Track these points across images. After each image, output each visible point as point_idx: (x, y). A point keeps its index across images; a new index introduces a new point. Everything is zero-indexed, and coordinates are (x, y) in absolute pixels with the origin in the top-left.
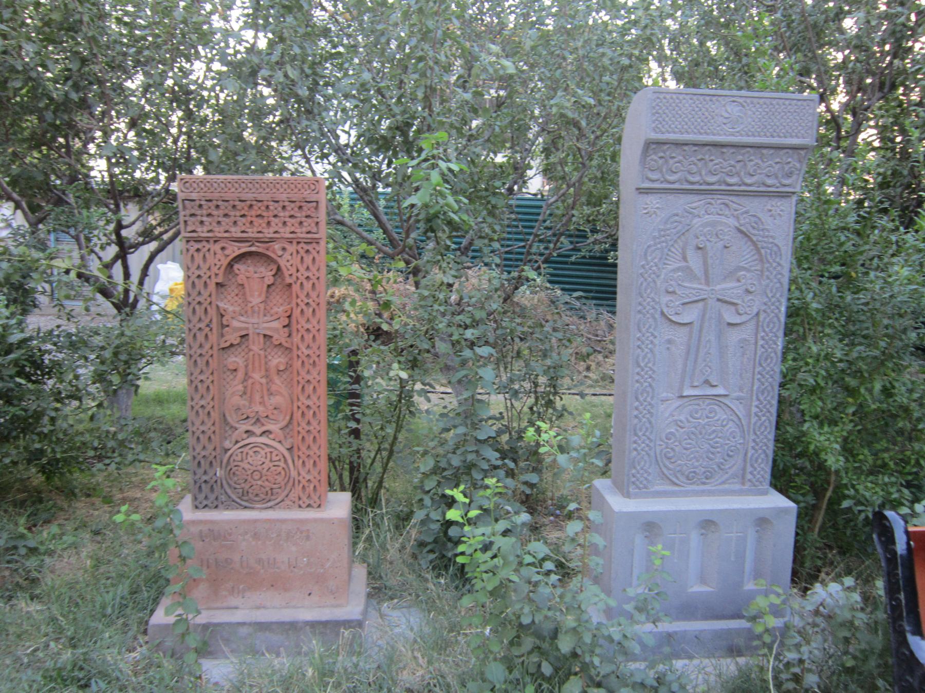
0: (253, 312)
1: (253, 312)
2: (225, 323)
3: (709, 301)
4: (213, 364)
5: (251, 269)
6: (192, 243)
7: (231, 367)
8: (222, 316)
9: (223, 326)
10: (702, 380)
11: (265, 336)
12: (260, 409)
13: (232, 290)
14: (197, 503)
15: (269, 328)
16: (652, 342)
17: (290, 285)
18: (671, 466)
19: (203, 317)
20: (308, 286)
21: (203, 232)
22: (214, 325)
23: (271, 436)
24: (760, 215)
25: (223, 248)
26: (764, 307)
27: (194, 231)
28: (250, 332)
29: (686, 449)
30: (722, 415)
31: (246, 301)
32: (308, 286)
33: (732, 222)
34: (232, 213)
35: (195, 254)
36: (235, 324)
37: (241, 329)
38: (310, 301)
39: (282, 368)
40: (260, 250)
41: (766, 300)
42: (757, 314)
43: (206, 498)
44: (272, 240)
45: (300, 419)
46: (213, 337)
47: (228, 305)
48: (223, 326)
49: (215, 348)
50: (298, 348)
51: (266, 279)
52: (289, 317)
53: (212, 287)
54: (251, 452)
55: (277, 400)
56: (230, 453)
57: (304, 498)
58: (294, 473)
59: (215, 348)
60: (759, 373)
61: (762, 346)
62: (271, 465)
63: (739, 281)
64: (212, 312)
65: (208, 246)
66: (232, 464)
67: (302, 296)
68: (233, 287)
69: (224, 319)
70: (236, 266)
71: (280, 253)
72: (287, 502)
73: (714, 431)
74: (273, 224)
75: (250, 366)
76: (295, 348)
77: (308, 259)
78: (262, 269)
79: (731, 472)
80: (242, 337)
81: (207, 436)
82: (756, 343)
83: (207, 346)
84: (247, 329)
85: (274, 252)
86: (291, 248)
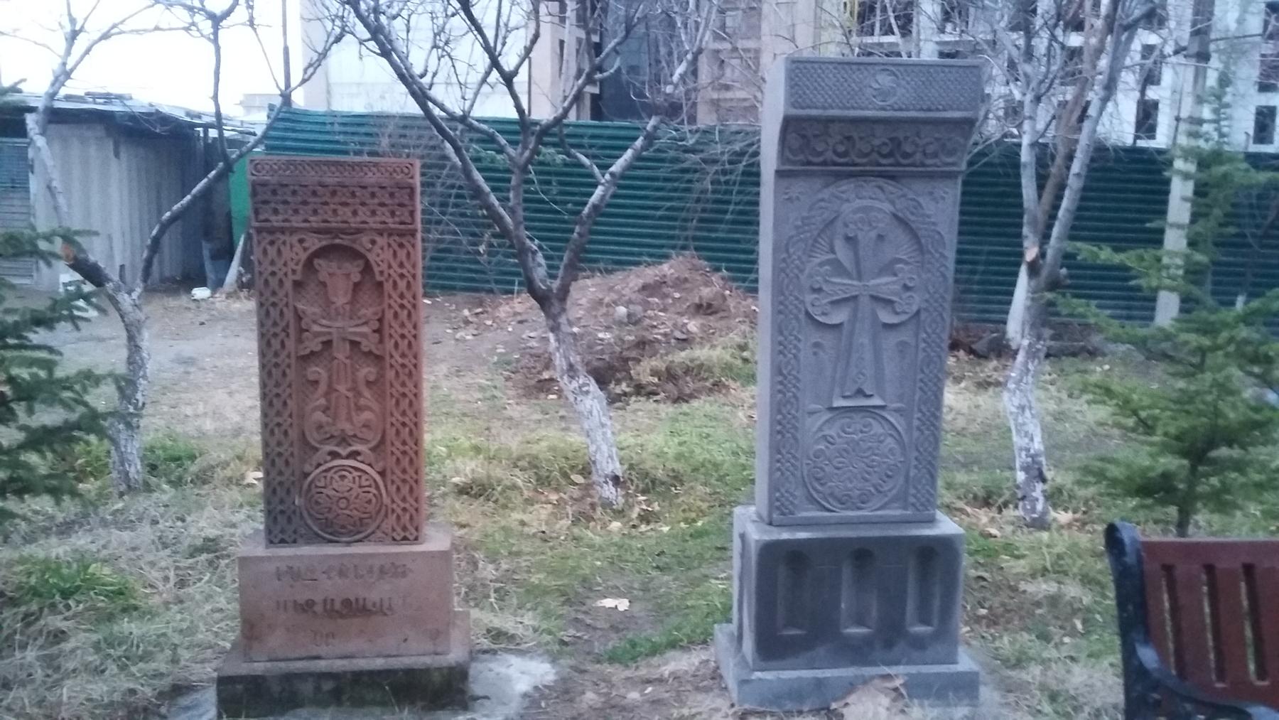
0: (338, 314)
2: (304, 327)
3: (861, 299)
5: (334, 264)
6: (264, 234)
7: (311, 378)
8: (300, 319)
9: (302, 331)
10: (855, 388)
12: (347, 427)
15: (355, 334)
16: (795, 347)
17: (380, 284)
18: (819, 488)
20: (402, 285)
21: (276, 221)
22: (292, 331)
24: (921, 200)
26: (924, 305)
27: (267, 220)
28: (335, 337)
29: (838, 468)
30: (877, 428)
31: (329, 303)
32: (402, 285)
33: (887, 207)
34: (312, 200)
35: (269, 247)
36: (316, 328)
38: (405, 302)
39: (372, 378)
40: (345, 243)
41: (927, 296)
42: (918, 313)
43: (282, 531)
44: (359, 231)
45: (394, 438)
46: (290, 344)
48: (302, 331)
50: (392, 356)
53: (288, 284)
55: (366, 415)
56: (310, 479)
57: (399, 530)
58: (386, 500)
59: (293, 355)
60: (921, 380)
61: (924, 350)
62: (360, 490)
63: (895, 275)
64: (289, 315)
65: (283, 238)
66: (314, 490)
67: (395, 296)
70: (316, 261)
72: (379, 534)
73: (870, 448)
74: (360, 213)
75: (334, 378)
76: (387, 358)
77: (402, 254)
78: (347, 265)
79: (890, 495)
80: (323, 343)
81: (283, 459)
82: (917, 346)
84: (330, 333)
85: (361, 244)
86: (381, 241)
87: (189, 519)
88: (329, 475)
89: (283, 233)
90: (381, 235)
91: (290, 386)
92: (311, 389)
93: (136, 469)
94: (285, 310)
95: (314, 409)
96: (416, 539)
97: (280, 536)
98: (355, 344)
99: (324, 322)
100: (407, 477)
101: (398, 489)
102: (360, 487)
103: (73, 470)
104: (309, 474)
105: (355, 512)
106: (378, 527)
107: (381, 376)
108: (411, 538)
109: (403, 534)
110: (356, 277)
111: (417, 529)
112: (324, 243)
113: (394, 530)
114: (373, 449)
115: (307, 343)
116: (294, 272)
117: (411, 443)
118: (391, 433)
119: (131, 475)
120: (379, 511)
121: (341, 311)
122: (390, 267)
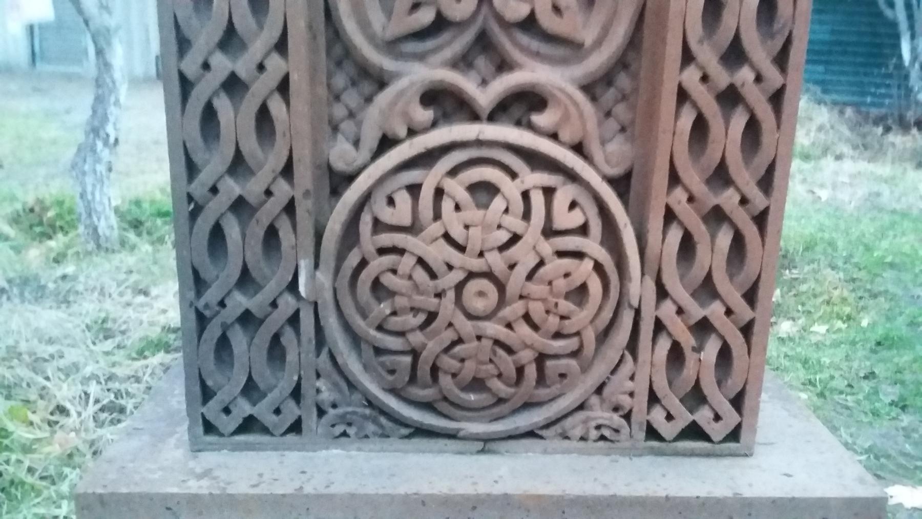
14: (212, 410)
23: (541, 119)
43: (251, 389)
54: (456, 188)
58: (640, 288)
62: (547, 248)
72: (600, 414)
87: (154, 291)
88: (430, 178)
93: (108, 225)
96: (734, 435)
97: (244, 408)
100: (729, 199)
101: (687, 246)
102: (549, 232)
103: (41, 223)
104: (350, 178)
105: (524, 329)
106: (599, 390)
108: (717, 431)
109: (684, 418)
111: (737, 402)
113: (653, 399)
114: (590, 88)
119: (100, 231)
120: (604, 335)
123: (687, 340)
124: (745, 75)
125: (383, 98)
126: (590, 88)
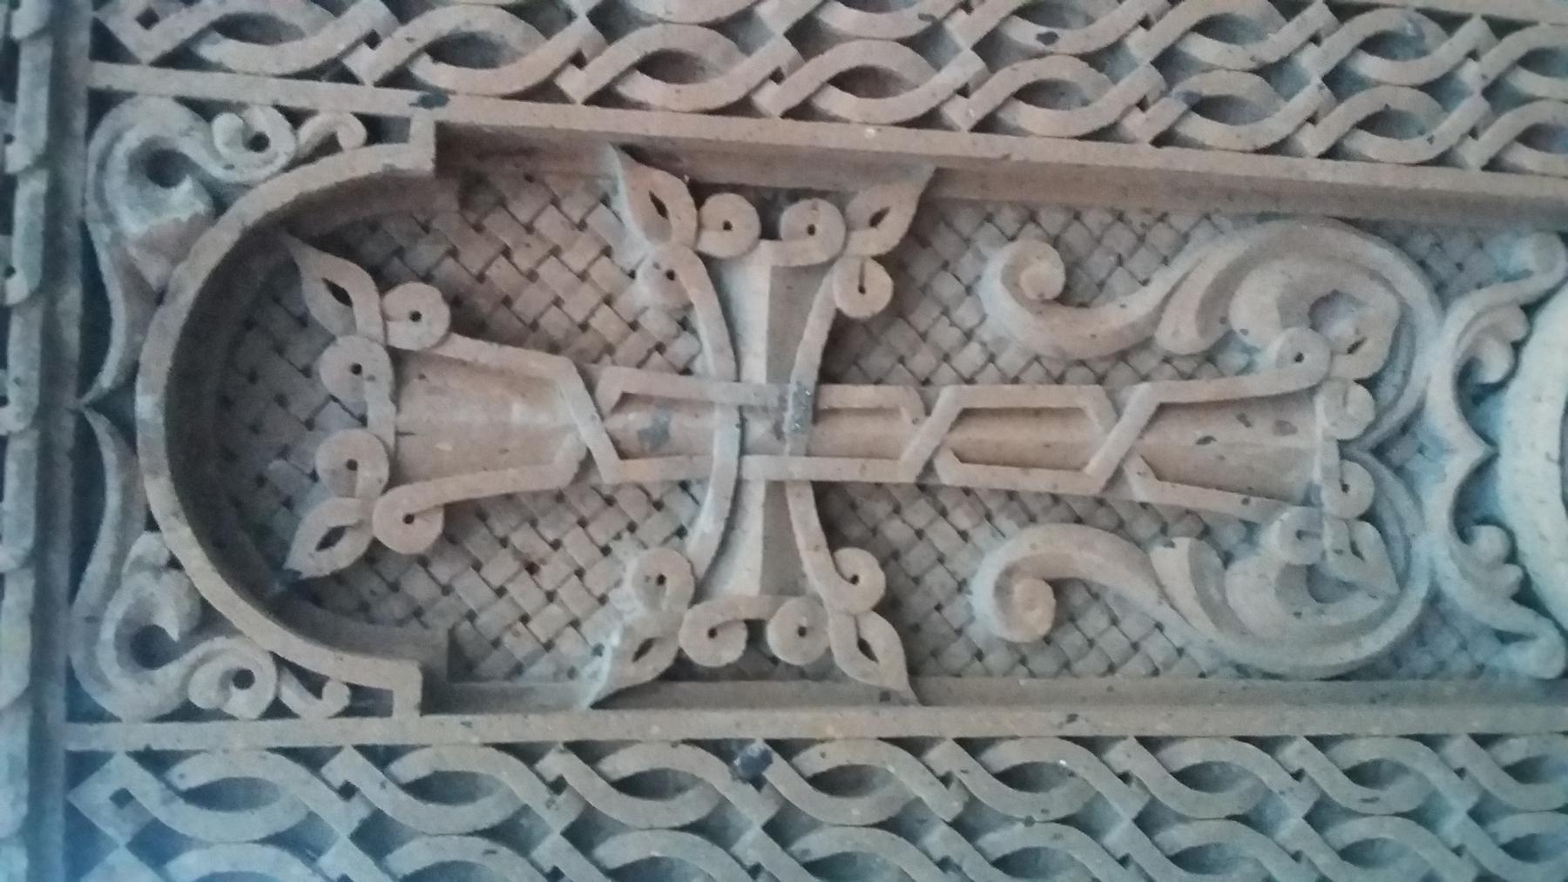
0: (656, 442)
1: (656, 442)
2: (731, 650)
4: (1029, 733)
7: (1038, 616)
8: (682, 669)
9: (758, 663)
11: (828, 375)
12: (1324, 425)
13: (480, 592)
15: (779, 367)
19: (690, 808)
22: (755, 725)
25: (146, 648)
36: (743, 578)
37: (779, 543)
39: (1048, 272)
47: (611, 615)
48: (758, 663)
49: (915, 721)
51: (405, 336)
52: (700, 192)
53: (452, 741)
55: (1255, 310)
59: (915, 721)
68: (472, 592)
69: (704, 654)
70: (306, 559)
71: (184, 200)
75: (1038, 482)
78: (331, 368)
80: (834, 536)
83: (909, 779)
84: (776, 489)
85: (180, 246)
86: (151, 110)
89: (84, 765)
90: (102, 102)
91: (1094, 745)
92: (1094, 621)
94: (623, 764)
95: (1218, 611)
98: (844, 353)
99: (706, 527)
107: (1026, 201)
110: (417, 317)
112: (159, 493)
115: (837, 639)
116: (364, 702)
117: (1445, 52)
118: (1384, 163)
121: (635, 421)
122: (336, 71)
123: (1513, 121)
124: (1472, 75)
125: (1461, 594)
126: (1442, 293)
